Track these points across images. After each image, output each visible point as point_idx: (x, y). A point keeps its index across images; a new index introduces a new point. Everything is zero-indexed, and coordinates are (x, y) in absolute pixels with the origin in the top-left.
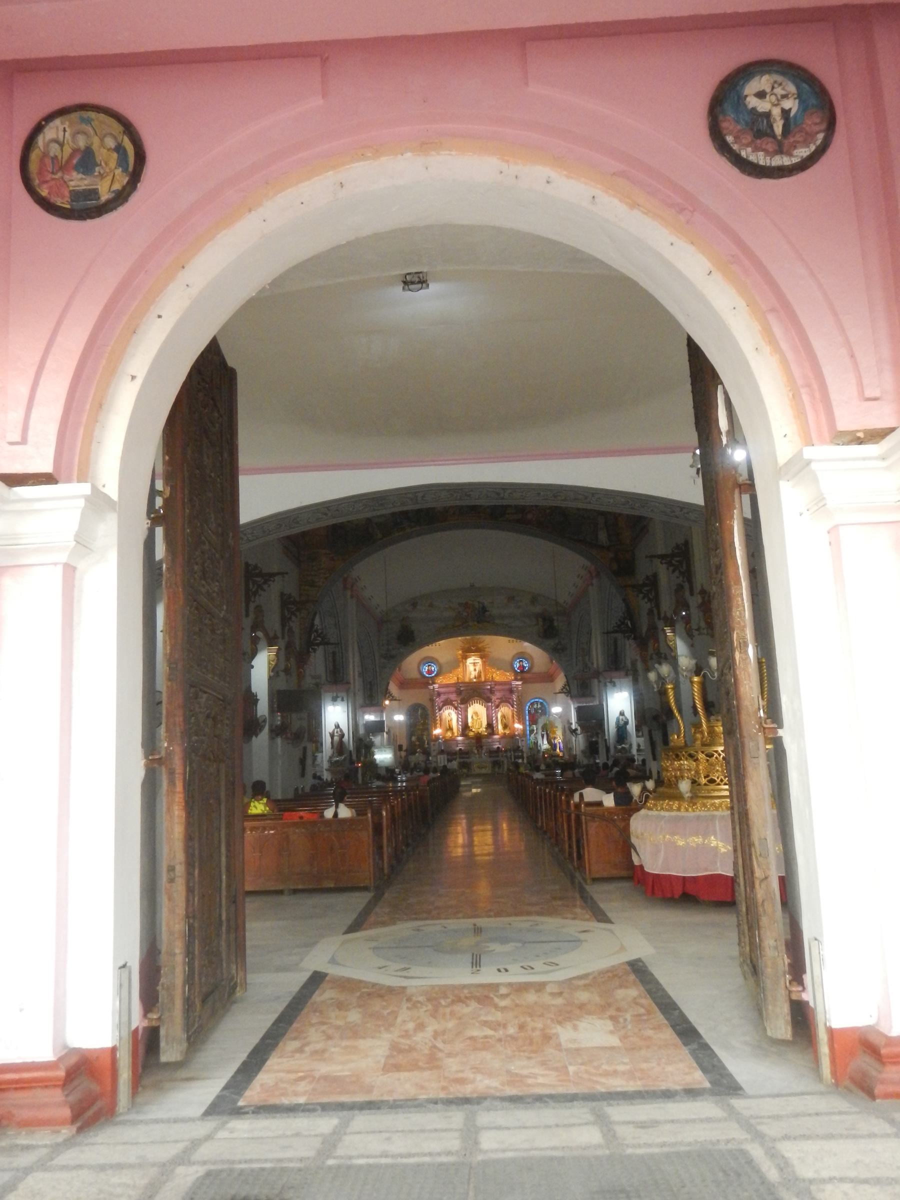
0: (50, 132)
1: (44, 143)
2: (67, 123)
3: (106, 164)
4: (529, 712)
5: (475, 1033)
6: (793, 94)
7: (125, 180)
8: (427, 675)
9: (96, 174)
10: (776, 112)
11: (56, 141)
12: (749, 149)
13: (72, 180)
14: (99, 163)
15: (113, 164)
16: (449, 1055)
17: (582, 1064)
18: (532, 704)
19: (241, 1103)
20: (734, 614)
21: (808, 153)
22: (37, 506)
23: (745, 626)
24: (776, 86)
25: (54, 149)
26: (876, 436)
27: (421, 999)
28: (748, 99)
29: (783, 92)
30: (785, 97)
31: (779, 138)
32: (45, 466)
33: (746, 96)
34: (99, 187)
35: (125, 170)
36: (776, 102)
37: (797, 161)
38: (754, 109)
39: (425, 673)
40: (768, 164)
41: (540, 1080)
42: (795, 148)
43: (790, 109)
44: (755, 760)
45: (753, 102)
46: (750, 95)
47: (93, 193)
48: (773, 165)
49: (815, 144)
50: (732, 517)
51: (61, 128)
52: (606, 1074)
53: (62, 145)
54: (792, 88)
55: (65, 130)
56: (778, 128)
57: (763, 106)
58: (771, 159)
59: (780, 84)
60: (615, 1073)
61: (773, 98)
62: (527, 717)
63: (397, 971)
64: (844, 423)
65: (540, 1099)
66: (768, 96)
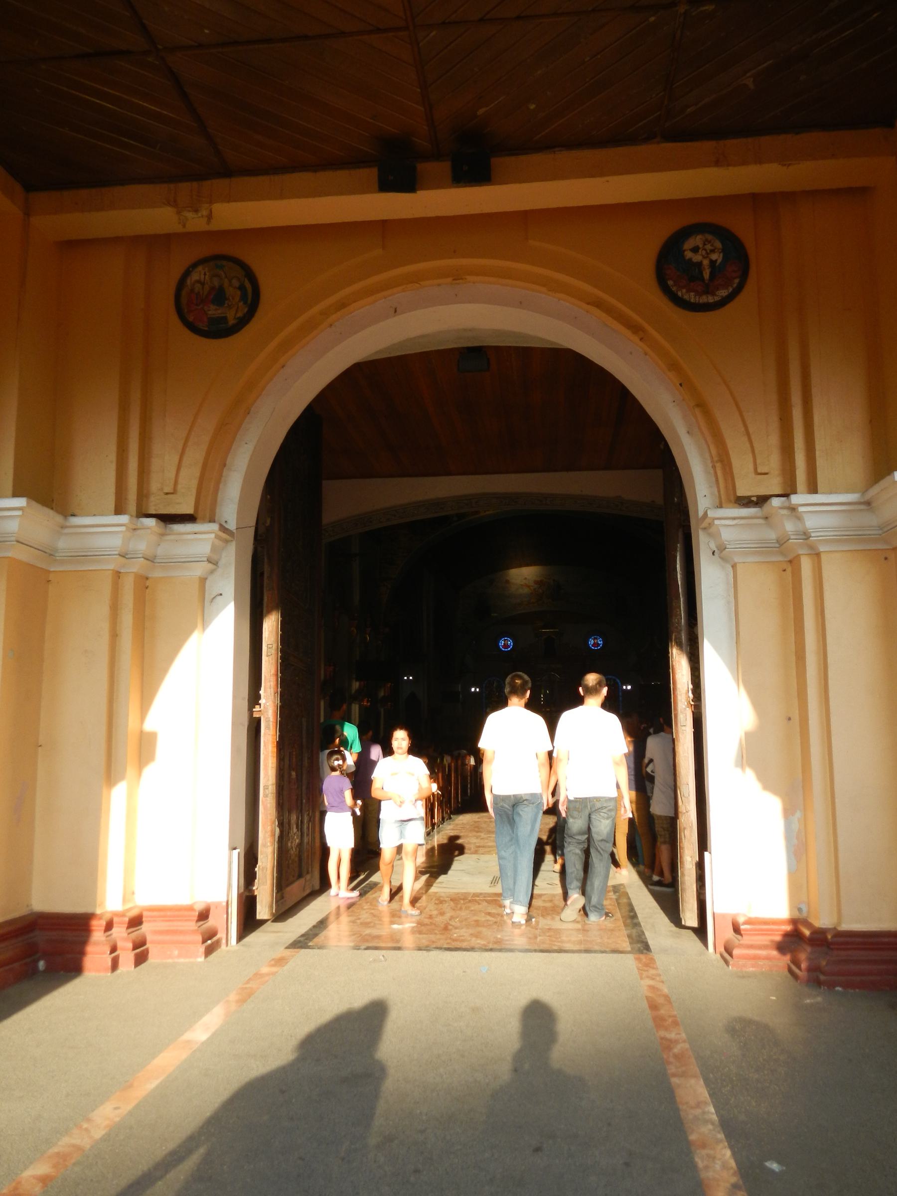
0: (195, 276)
2: (207, 269)
6: (719, 249)
7: (246, 310)
8: (503, 649)
9: (226, 305)
10: (706, 262)
11: (199, 282)
12: (684, 291)
13: (209, 310)
20: (673, 621)
21: (726, 294)
22: (185, 537)
23: (681, 630)
24: (706, 243)
25: (198, 287)
26: (761, 501)
27: (446, 899)
28: (686, 253)
29: (712, 248)
30: (713, 251)
31: (707, 282)
32: (188, 509)
33: (684, 251)
34: (228, 315)
35: (245, 303)
36: (706, 256)
37: (718, 299)
38: (690, 260)
39: (501, 647)
40: (697, 302)
42: (718, 289)
43: (716, 260)
44: (684, 728)
45: (689, 255)
46: (687, 250)
47: (224, 319)
48: (700, 302)
49: (732, 286)
50: (676, 550)
51: (203, 273)
54: (718, 245)
55: (205, 274)
56: (706, 275)
57: (697, 258)
58: (699, 298)
59: (709, 242)
60: (569, 941)
61: (704, 252)
64: (743, 491)
66: (700, 251)
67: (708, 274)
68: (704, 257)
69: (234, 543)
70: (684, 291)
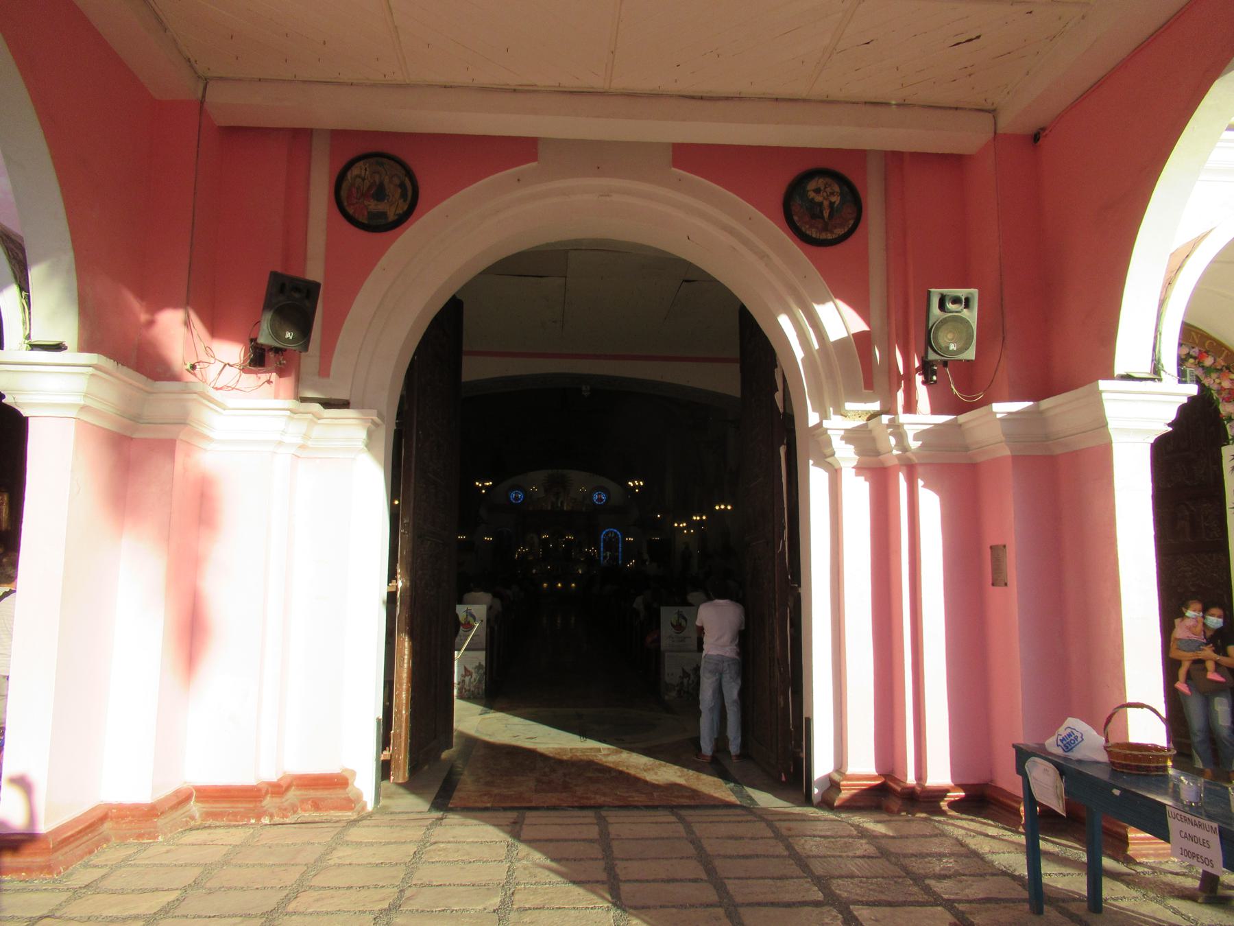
0: (355, 171)
1: (351, 178)
2: (367, 165)
3: (393, 196)
4: (604, 540)
5: (590, 775)
7: (405, 208)
8: (514, 501)
9: (386, 201)
10: (826, 203)
11: (358, 176)
12: (807, 226)
14: (387, 194)
15: (397, 195)
16: (576, 786)
17: (662, 792)
18: (607, 533)
19: (450, 806)
29: (831, 191)
30: (832, 194)
33: (808, 191)
35: (405, 201)
41: (636, 799)
42: (835, 227)
43: (834, 202)
45: (812, 195)
52: (677, 797)
53: (364, 179)
54: (837, 189)
55: (366, 170)
56: (826, 215)
57: (818, 199)
59: (830, 185)
61: (825, 194)
62: (602, 544)
63: (527, 738)
65: (636, 807)
67: (827, 215)
68: (824, 198)
69: (384, 426)
70: (807, 226)
